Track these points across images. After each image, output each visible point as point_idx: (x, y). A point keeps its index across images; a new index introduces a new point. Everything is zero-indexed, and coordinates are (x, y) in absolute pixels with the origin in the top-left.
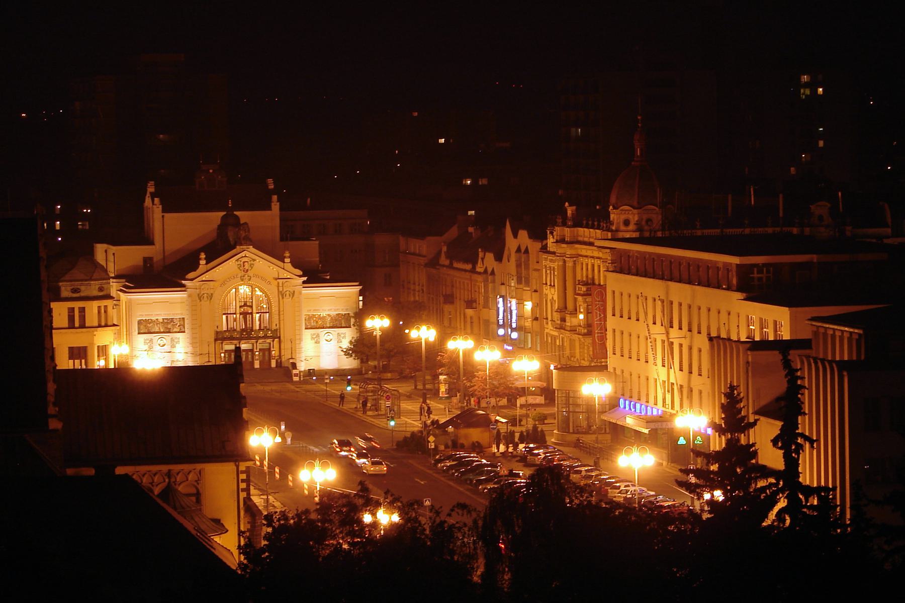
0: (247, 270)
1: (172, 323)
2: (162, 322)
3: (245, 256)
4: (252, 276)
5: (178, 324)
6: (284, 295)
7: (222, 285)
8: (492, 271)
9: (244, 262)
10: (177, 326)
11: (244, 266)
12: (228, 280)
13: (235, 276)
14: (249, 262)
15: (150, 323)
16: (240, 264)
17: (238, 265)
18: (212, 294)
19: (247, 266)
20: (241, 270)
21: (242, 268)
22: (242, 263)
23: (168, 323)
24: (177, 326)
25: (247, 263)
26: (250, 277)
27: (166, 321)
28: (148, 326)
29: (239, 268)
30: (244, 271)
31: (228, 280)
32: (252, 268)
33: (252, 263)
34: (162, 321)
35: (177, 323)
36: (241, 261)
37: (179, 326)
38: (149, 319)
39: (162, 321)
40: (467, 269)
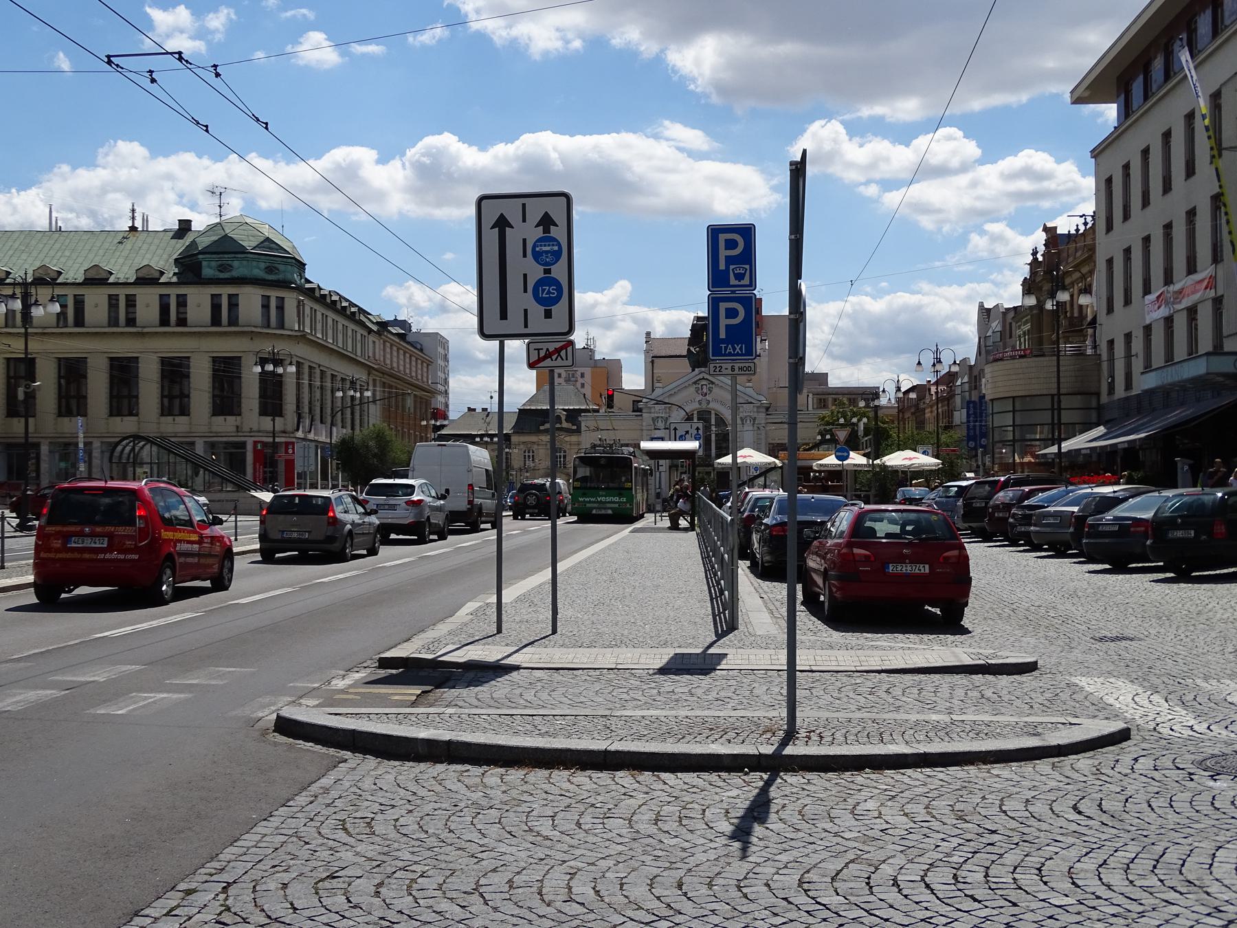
3: (703, 378)
8: (1092, 319)
9: (702, 385)
11: (702, 389)
19: (705, 390)
21: (700, 392)
22: (700, 386)
32: (711, 391)
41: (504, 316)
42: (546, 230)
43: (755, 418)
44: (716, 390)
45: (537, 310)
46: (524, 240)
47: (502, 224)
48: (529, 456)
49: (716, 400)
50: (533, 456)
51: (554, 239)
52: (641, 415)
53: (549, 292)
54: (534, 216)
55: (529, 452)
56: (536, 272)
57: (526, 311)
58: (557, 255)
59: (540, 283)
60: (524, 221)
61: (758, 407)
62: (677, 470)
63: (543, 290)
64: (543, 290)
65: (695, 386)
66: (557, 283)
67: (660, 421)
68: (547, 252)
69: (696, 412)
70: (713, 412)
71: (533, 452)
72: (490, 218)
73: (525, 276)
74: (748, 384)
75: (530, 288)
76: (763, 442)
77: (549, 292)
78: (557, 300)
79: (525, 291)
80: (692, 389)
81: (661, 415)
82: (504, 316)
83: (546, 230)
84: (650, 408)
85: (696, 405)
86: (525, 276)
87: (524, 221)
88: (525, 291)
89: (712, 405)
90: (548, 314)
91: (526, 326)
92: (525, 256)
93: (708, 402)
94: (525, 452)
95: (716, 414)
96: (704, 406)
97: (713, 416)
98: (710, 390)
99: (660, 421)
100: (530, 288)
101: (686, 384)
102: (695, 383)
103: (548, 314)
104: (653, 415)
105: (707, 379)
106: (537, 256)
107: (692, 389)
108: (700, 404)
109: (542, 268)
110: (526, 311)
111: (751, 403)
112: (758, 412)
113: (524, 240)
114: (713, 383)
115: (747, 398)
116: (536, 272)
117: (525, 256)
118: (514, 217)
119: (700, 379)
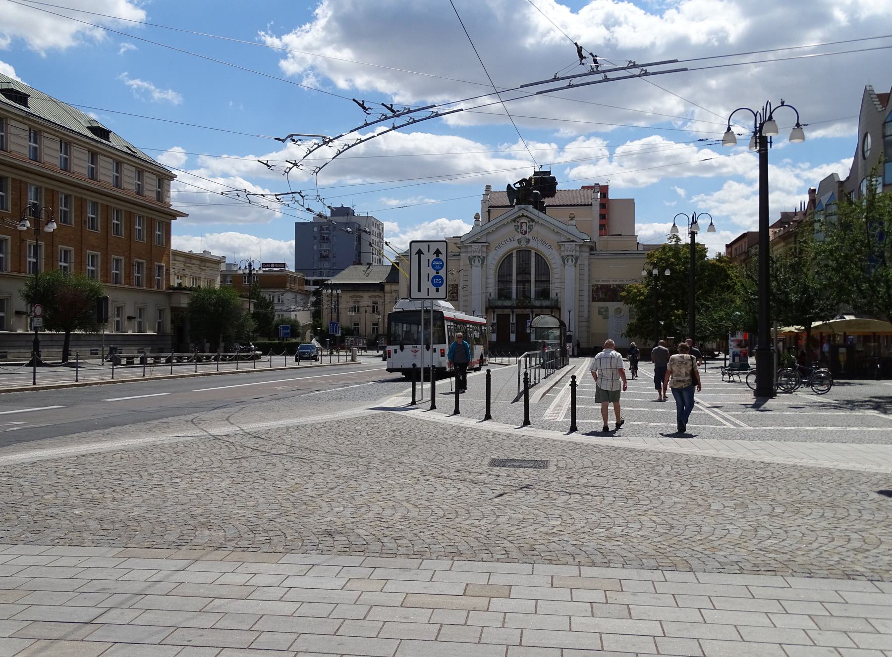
0: (525, 233)
3: (523, 216)
4: (531, 239)
7: (497, 248)
9: (522, 223)
11: (521, 228)
12: (504, 243)
13: (512, 239)
14: (528, 224)
16: (518, 226)
17: (515, 226)
19: (524, 228)
20: (518, 232)
21: (519, 230)
22: (519, 224)
26: (529, 240)
29: (516, 230)
30: (522, 233)
32: (531, 230)
33: (531, 224)
36: (518, 222)
41: (419, 290)
42: (438, 256)
43: (577, 259)
44: (536, 228)
45: (434, 289)
46: (429, 260)
47: (420, 253)
49: (537, 239)
51: (440, 260)
53: (438, 281)
54: (433, 250)
56: (433, 273)
57: (428, 289)
58: (442, 266)
59: (434, 277)
60: (429, 251)
61: (581, 246)
62: (494, 312)
66: (441, 277)
67: (477, 261)
69: (515, 252)
70: (533, 251)
72: (414, 251)
73: (428, 274)
74: (571, 222)
77: (438, 281)
78: (441, 285)
79: (428, 280)
80: (511, 227)
81: (476, 254)
82: (419, 290)
83: (438, 256)
84: (467, 247)
85: (515, 244)
86: (428, 274)
88: (428, 280)
89: (533, 244)
90: (437, 290)
92: (428, 266)
93: (528, 241)
95: (536, 253)
96: (524, 245)
97: (533, 255)
98: (531, 229)
101: (505, 222)
102: (514, 220)
103: (437, 290)
105: (526, 216)
106: (433, 266)
107: (511, 227)
108: (519, 243)
110: (428, 289)
111: (573, 241)
112: (581, 251)
113: (429, 260)
114: (533, 221)
115: (569, 236)
116: (433, 273)
117: (428, 266)
118: (425, 250)
119: (519, 217)
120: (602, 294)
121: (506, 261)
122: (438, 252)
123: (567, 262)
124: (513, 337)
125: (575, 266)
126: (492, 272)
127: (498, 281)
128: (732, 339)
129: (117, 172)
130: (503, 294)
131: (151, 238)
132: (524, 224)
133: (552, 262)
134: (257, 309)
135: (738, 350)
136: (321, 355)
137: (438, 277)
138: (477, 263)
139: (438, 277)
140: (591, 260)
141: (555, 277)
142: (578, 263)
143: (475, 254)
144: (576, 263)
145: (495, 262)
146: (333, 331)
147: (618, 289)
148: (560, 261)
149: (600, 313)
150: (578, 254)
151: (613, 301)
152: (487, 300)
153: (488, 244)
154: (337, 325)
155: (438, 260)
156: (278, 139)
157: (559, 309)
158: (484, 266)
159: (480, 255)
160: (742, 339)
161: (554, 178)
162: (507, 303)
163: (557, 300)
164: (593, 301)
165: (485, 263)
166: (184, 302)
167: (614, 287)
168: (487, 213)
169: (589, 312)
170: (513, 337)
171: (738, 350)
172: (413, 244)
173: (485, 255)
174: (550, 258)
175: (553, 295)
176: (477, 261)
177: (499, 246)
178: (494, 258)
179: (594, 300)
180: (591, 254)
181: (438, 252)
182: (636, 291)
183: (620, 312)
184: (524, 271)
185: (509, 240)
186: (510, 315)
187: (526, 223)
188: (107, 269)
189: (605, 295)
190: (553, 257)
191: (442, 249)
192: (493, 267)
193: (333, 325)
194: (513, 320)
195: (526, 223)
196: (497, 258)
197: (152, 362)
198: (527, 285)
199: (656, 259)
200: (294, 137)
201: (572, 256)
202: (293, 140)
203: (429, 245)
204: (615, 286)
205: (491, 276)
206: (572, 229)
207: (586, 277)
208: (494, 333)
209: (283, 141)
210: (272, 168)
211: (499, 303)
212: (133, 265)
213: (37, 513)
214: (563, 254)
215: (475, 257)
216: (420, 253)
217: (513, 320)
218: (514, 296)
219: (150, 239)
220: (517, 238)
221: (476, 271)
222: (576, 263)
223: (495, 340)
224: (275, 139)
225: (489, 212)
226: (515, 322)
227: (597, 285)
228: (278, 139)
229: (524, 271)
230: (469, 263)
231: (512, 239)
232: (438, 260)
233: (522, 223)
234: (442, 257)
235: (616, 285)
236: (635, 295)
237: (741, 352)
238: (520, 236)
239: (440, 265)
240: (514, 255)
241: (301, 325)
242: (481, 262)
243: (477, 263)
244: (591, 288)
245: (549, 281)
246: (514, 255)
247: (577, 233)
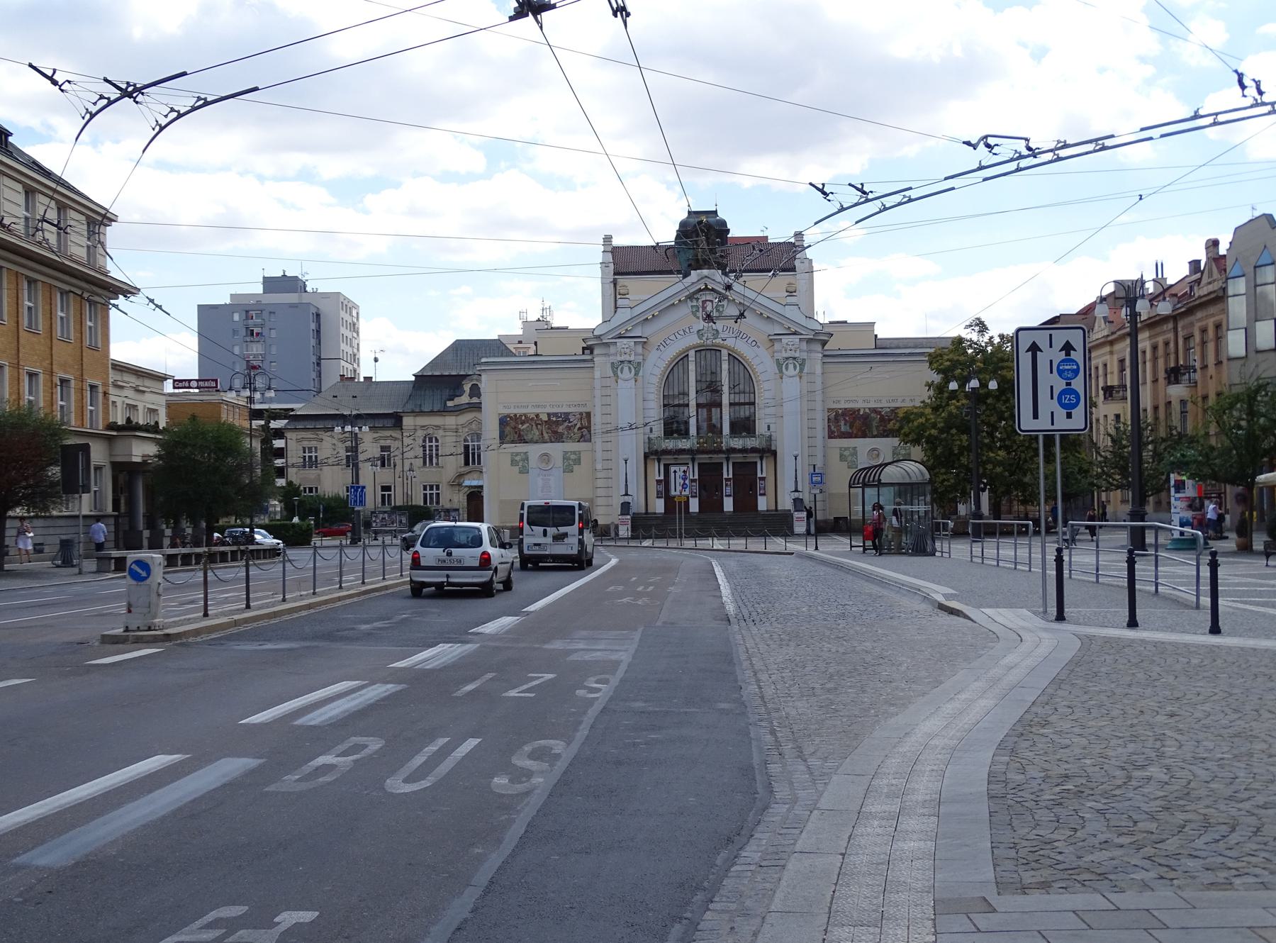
1: (566, 424)
2: (546, 422)
3: (706, 289)
4: (720, 331)
5: (579, 425)
6: (784, 366)
10: (576, 430)
12: (673, 337)
15: (523, 423)
18: (639, 363)
20: (698, 318)
23: (557, 423)
24: (576, 430)
25: (708, 303)
26: (717, 331)
27: (554, 419)
28: (520, 430)
29: (694, 314)
31: (673, 337)
34: (546, 419)
35: (575, 422)
36: (697, 299)
37: (579, 429)
38: (521, 416)
39: (546, 419)
40: (1106, 334)
41: (1036, 416)
42: (1068, 354)
43: (802, 365)
45: (1061, 413)
46: (1051, 361)
47: (1034, 349)
48: (430, 446)
50: (437, 446)
51: (1073, 361)
52: (592, 360)
53: (1070, 400)
55: (431, 441)
56: (1060, 385)
57: (1052, 413)
58: (1076, 372)
59: (1063, 393)
60: (1051, 346)
61: (809, 341)
62: (659, 462)
63: (1065, 398)
64: (1065, 398)
65: (690, 304)
67: (626, 369)
68: (1068, 370)
69: (692, 353)
70: (725, 353)
71: (437, 440)
72: (1024, 344)
73: (1052, 387)
74: (790, 300)
75: (1055, 396)
76: (819, 406)
77: (1070, 400)
79: (1052, 398)
80: (685, 310)
81: (627, 358)
82: (1036, 416)
83: (1068, 354)
84: (607, 345)
85: (694, 340)
86: (1052, 387)
87: (1051, 346)
88: (1052, 398)
90: (1069, 416)
91: (1053, 424)
92: (1051, 372)
94: (424, 441)
95: (729, 354)
99: (626, 369)
100: (1055, 396)
102: (691, 297)
103: (1069, 416)
104: (613, 359)
105: (713, 290)
106: (1060, 373)
109: (1065, 381)
110: (1052, 413)
111: (795, 333)
112: (809, 351)
113: (1051, 361)
115: (787, 325)
116: (1060, 385)
117: (1051, 372)
118: (1042, 344)
119: (700, 290)
120: (845, 424)
121: (675, 369)
122: (1068, 348)
123: (787, 369)
124: (728, 504)
125: (800, 377)
126: (653, 389)
127: (665, 406)
128: (1178, 495)
129: (27, 210)
130: (674, 427)
131: (81, 333)
132: (709, 304)
133: (759, 369)
134: (1065, 452)
135: (1188, 515)
136: (384, 546)
137: (1068, 391)
138: (626, 374)
139: (1068, 391)
140: (826, 366)
141: (764, 394)
142: (805, 371)
143: (622, 358)
144: (801, 370)
145: (658, 372)
146: (355, 501)
147: (873, 415)
148: (771, 367)
149: (842, 458)
150: (804, 355)
151: (864, 436)
152: (647, 441)
153: (645, 340)
154: (362, 491)
155: (1068, 360)
156: (968, 143)
157: (774, 454)
158: (640, 379)
159: (632, 358)
160: (1196, 495)
161: (724, 223)
162: (684, 444)
163: (770, 436)
164: (830, 437)
165: (641, 374)
166: (142, 450)
167: (865, 413)
168: (612, 285)
169: (824, 456)
170: (728, 504)
171: (1188, 515)
172: (1020, 333)
173: (640, 359)
174: (755, 362)
175: (761, 428)
176: (791, 366)
177: (665, 344)
178: (657, 364)
179: (831, 435)
180: (824, 356)
181: (1068, 348)
182: (922, 420)
183: (878, 455)
184: (711, 387)
185: (682, 333)
186: (756, 463)
187: (712, 301)
188: (19, 393)
189: (851, 428)
190: (761, 361)
191: (1076, 338)
192: (655, 380)
193: (356, 491)
194: (727, 472)
195: (712, 301)
196: (663, 365)
197: (94, 568)
198: (715, 411)
199: (948, 363)
200: (991, 141)
201: (794, 358)
202: (988, 146)
203: (1051, 335)
204: (867, 411)
205: (652, 397)
206: (790, 312)
207: (819, 397)
208: (661, 497)
209: (975, 147)
210: (830, 197)
211: (670, 444)
212: (56, 387)
213: (1233, 830)
214: (778, 356)
215: (622, 362)
216: (1034, 349)
217: (727, 472)
218: (693, 430)
219: (79, 335)
220: (695, 329)
221: (626, 388)
222: (801, 370)
223: (662, 511)
224: (964, 143)
225: (615, 283)
226: (731, 476)
227: (836, 410)
228: (968, 143)
229: (711, 387)
230: (612, 375)
231: (687, 330)
232: (1068, 360)
233: (704, 302)
234: (1077, 356)
235: (869, 409)
236: (922, 427)
237: (1194, 518)
238: (702, 324)
239: (1073, 371)
240: (692, 358)
241: (343, 493)
242: (798, 368)
243: (626, 374)
244: (827, 414)
245: (754, 404)
246: (692, 358)
247: (803, 321)
